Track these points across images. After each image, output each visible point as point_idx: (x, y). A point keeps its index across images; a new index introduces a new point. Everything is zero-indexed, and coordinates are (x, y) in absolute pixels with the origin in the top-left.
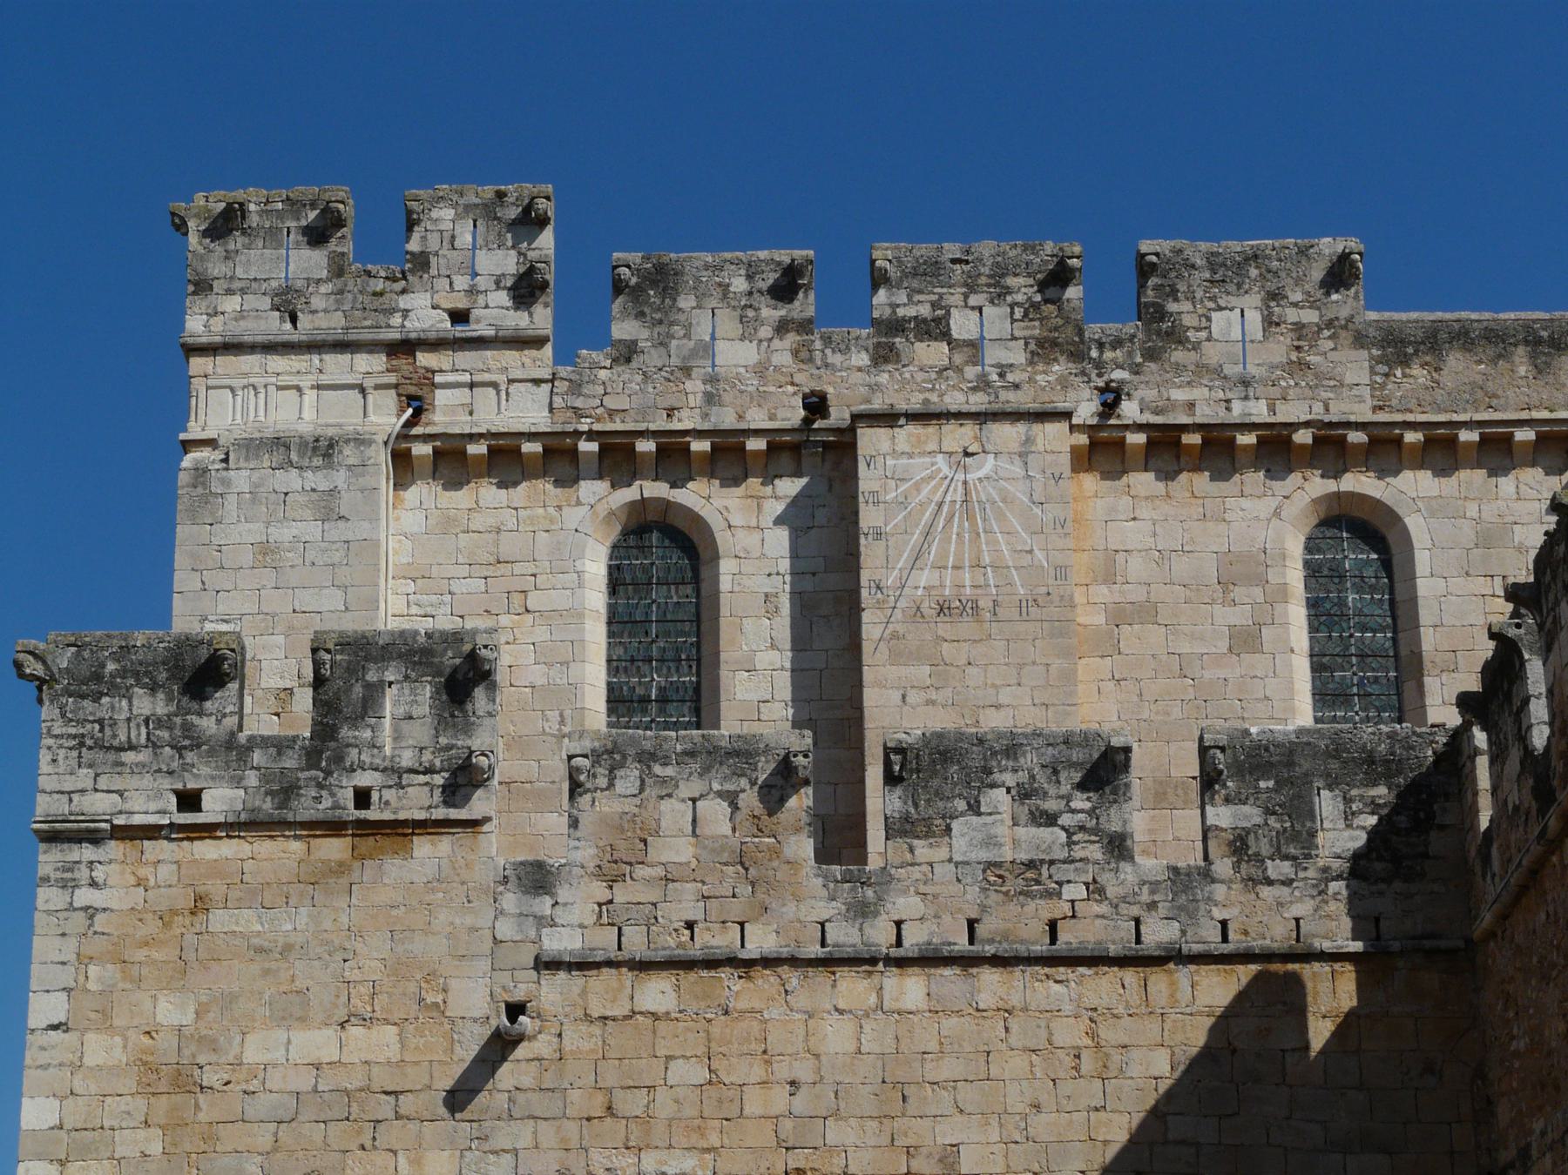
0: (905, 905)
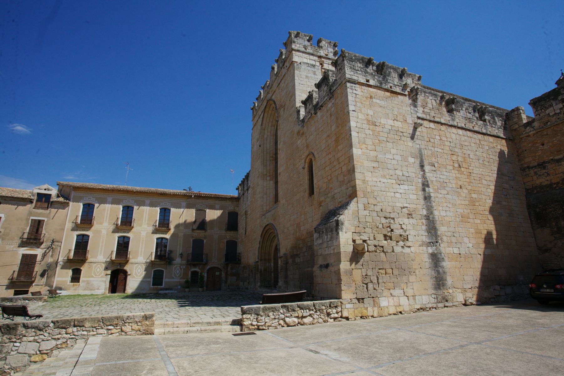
0: (457, 120)
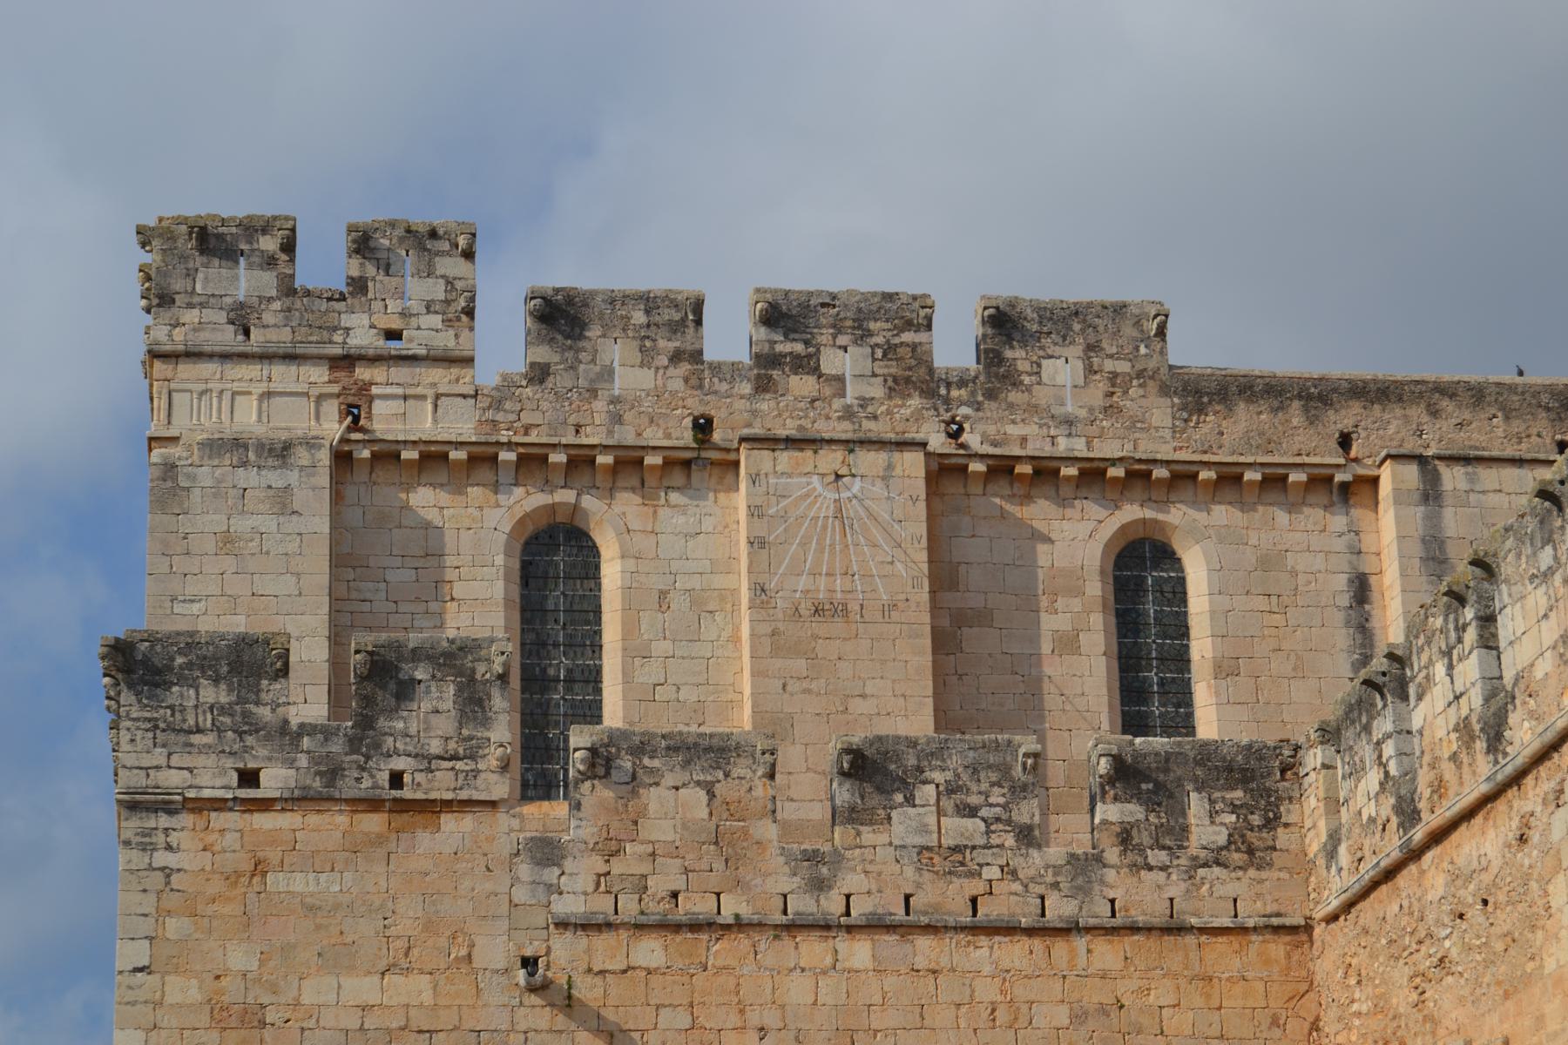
0: (852, 881)
